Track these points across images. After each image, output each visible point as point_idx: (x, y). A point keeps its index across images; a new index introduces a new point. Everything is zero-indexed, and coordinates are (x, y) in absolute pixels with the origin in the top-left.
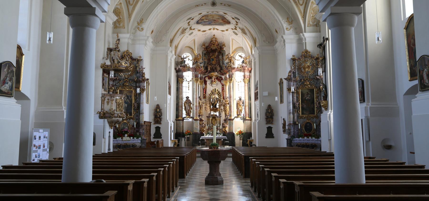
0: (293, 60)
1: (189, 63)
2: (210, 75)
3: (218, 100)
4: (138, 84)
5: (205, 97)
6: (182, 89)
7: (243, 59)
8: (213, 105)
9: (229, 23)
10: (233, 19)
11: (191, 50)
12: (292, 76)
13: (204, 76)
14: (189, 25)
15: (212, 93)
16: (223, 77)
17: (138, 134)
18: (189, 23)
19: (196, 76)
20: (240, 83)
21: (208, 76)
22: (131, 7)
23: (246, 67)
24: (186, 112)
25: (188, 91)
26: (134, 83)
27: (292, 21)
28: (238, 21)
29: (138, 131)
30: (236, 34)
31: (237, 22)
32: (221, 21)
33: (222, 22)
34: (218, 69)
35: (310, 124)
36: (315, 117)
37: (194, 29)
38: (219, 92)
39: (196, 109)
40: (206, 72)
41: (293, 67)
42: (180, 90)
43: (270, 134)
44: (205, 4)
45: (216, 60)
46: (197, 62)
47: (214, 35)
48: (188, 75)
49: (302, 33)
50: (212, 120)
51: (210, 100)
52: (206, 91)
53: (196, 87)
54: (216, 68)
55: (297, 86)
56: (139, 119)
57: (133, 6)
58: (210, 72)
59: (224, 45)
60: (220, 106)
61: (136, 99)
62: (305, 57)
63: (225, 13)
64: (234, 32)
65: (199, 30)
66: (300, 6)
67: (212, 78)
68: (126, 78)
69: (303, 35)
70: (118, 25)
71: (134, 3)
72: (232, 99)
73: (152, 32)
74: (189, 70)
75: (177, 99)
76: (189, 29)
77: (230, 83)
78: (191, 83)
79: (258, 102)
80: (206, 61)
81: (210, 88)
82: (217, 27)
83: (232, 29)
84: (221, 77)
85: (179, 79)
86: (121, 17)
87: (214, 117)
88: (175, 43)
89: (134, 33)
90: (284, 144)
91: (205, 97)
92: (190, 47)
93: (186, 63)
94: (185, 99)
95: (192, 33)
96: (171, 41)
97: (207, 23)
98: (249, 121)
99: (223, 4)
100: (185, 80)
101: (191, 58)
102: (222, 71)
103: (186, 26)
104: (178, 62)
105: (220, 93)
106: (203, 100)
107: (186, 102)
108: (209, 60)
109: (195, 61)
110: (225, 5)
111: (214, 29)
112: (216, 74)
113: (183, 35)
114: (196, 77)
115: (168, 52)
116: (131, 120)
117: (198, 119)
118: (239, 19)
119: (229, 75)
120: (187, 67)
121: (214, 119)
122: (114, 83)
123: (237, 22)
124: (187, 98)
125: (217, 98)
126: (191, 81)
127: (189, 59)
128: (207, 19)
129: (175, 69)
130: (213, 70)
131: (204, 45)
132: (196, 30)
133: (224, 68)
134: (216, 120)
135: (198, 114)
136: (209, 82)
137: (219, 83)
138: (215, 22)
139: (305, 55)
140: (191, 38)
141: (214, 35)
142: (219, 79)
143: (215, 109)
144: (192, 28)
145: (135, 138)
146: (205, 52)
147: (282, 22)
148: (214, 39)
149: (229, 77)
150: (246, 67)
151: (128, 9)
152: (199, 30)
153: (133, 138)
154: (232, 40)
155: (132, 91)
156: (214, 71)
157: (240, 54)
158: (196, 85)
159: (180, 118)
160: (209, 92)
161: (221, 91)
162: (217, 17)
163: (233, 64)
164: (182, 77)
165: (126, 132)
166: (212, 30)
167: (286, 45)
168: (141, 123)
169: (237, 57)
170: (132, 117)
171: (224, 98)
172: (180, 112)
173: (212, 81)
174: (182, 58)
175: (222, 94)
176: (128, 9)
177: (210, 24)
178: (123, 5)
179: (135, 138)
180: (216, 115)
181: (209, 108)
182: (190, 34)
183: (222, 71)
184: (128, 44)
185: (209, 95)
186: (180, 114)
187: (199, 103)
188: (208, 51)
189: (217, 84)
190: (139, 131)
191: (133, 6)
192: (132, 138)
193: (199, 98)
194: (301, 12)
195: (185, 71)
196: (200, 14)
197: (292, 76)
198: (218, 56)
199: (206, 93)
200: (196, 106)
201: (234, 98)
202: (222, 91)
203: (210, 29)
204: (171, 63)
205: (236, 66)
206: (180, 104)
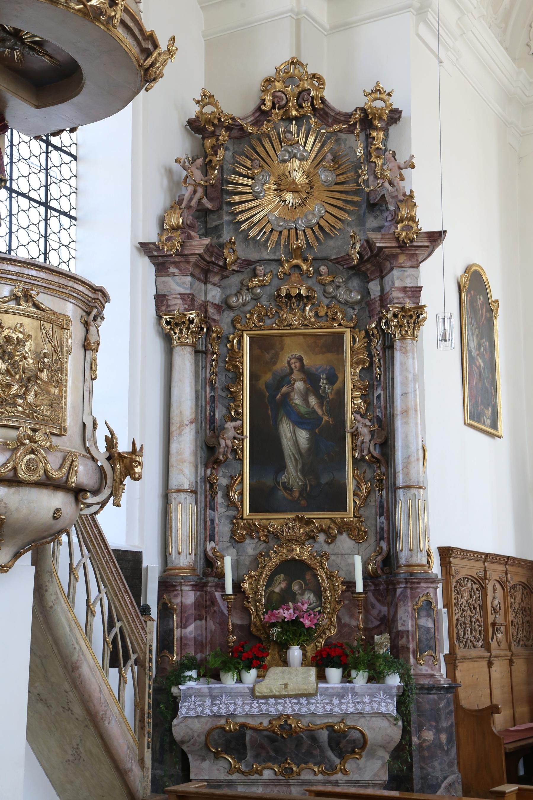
4: (374, 287)
17: (382, 642)
26: (355, 283)
29: (388, 624)
56: (388, 534)
61: (371, 388)
68: (293, 253)
116: (345, 542)
122: (214, 294)
145: (360, 679)
153: (347, 678)
155: (340, 337)
165: (295, 631)
168: (403, 557)
170: (350, 514)
179: (360, 679)
184: (298, 22)
190: (394, 620)
192: (334, 674)
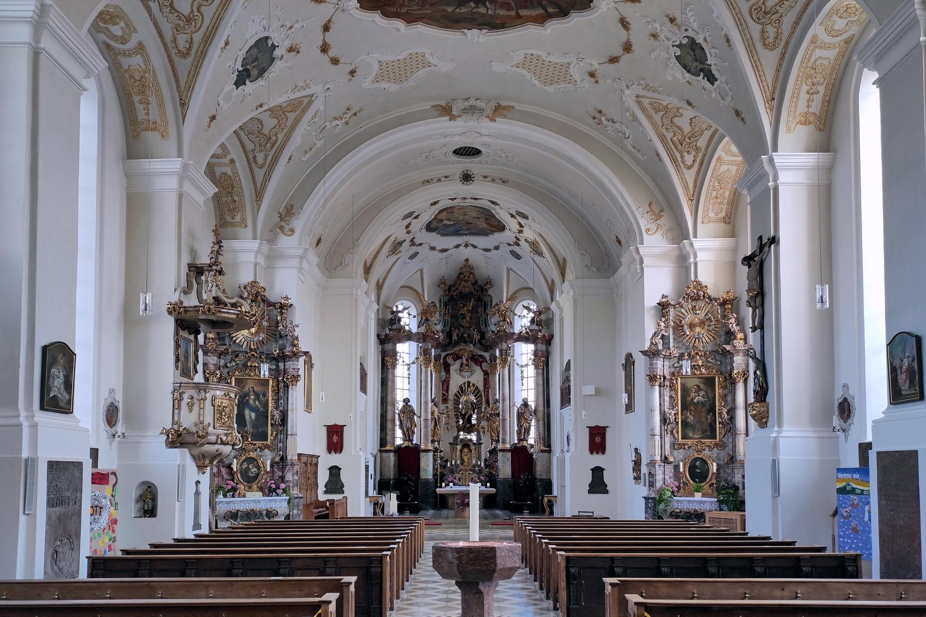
0: (663, 307)
1: (409, 321)
2: (457, 349)
3: (475, 407)
5: (445, 400)
6: (394, 382)
7: (532, 315)
8: (463, 418)
9: (501, 228)
10: (512, 216)
11: (418, 296)
12: (660, 347)
13: (443, 354)
14: (408, 232)
15: (461, 391)
16: (487, 355)
18: (407, 227)
19: (425, 352)
20: (525, 369)
22: (260, 174)
23: (540, 331)
24: (404, 434)
25: (405, 386)
27: (662, 211)
28: (523, 221)
30: (518, 257)
31: (521, 226)
32: (482, 224)
33: (485, 226)
34: (477, 337)
35: (704, 462)
36: (717, 445)
37: (421, 244)
38: (477, 388)
39: (426, 427)
40: (449, 344)
41: (662, 324)
42: (390, 384)
43: (598, 484)
44: (446, 177)
45: (471, 318)
46: (427, 320)
47: (467, 260)
48: (406, 351)
49: (687, 238)
51: (457, 408)
52: (448, 387)
53: (426, 377)
54: (470, 336)
55: (673, 370)
57: (264, 170)
58: (457, 343)
60: (478, 419)
62: (696, 298)
63: (493, 203)
64: (512, 252)
65: (433, 248)
66: (685, 170)
69: (692, 245)
70: (229, 219)
71: (268, 162)
73: (319, 241)
75: (382, 404)
76: (407, 244)
77: (503, 367)
78: (414, 368)
79: (569, 411)
80: (448, 318)
81: (456, 380)
82: (473, 240)
83: (509, 245)
84: (482, 356)
85: (387, 361)
86: (236, 198)
87: (466, 444)
88: (377, 273)
89: (272, 241)
90: (637, 512)
91: (445, 400)
92: (411, 288)
93: (402, 323)
94: (400, 405)
95: (416, 254)
96: (367, 270)
97: (451, 229)
98: (546, 454)
99: (489, 179)
100: (400, 361)
101: (414, 312)
102: (483, 341)
103: (401, 234)
104: (384, 320)
105: (479, 391)
106: (442, 407)
108: (454, 316)
109: (425, 317)
110: (493, 180)
111: (466, 246)
112: (471, 347)
113: (394, 258)
114: (425, 355)
115: (359, 293)
117: (431, 448)
118: (526, 217)
119: (501, 351)
120: (404, 331)
123: (521, 226)
124: (406, 401)
125: (472, 403)
126: (414, 363)
127: (409, 314)
128: (449, 220)
129: (378, 336)
130: (462, 340)
132: (426, 247)
133: (489, 335)
134: (470, 451)
136: (455, 367)
137: (477, 369)
138: (469, 226)
139: (693, 293)
140: (416, 264)
141: (467, 260)
142: (477, 360)
143: (469, 429)
144: (417, 241)
146: (446, 299)
147: (636, 213)
149: (501, 354)
150: (540, 331)
151: (253, 178)
152: (433, 248)
154: (508, 270)
156: (465, 342)
157: (525, 303)
158: (426, 372)
159: (388, 448)
161: (481, 388)
162: (474, 214)
163: (511, 324)
164: (394, 354)
166: (462, 248)
167: (646, 271)
169: (519, 310)
171: (488, 403)
172: (389, 433)
173: (462, 365)
174: (393, 313)
175: (484, 394)
176: (253, 178)
177: (457, 233)
178: (237, 164)
180: (471, 440)
182: (412, 257)
183: (483, 341)
186: (389, 438)
187: (432, 414)
188: (452, 296)
189: (472, 372)
191: (264, 170)
193: (433, 401)
194: (686, 187)
195: (400, 341)
196: (434, 204)
197: (660, 347)
199: (447, 391)
200: (426, 420)
203: (457, 246)
204: (367, 320)
205: (517, 330)
206: (389, 416)
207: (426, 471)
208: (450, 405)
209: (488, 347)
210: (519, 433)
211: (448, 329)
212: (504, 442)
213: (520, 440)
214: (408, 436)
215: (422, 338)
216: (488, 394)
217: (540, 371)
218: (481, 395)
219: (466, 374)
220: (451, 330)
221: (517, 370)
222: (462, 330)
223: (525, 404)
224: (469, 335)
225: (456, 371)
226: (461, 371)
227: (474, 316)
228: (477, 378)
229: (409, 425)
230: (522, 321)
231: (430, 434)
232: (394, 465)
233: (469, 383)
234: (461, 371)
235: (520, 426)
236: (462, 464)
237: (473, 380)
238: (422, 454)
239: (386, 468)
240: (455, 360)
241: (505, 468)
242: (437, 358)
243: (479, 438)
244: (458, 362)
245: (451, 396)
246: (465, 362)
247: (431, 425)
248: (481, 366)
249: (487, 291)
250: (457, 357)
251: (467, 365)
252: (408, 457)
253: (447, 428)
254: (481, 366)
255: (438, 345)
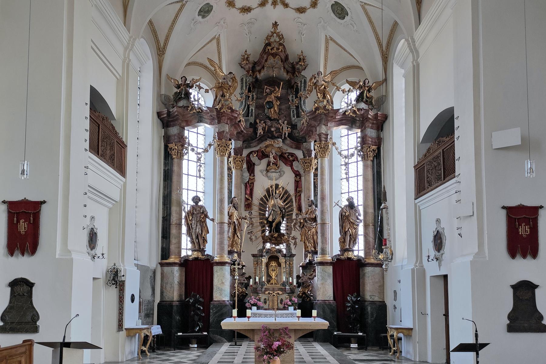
1: (202, 98)
2: (263, 145)
3: (285, 213)
5: (248, 206)
8: (270, 226)
15: (269, 194)
21: (257, 151)
24: (192, 242)
34: (286, 130)
38: (286, 192)
39: (221, 232)
42: (175, 178)
48: (199, 136)
50: (267, 265)
58: (262, 139)
59: (302, 59)
60: (288, 228)
67: (268, 156)
72: (327, 202)
74: (201, 120)
75: (164, 204)
81: (262, 183)
84: (292, 155)
87: (274, 257)
91: (248, 206)
98: (378, 269)
102: (296, 133)
105: (289, 195)
106: (245, 214)
107: (190, 213)
108: (260, 107)
109: (222, 89)
112: (279, 143)
114: (220, 139)
121: (273, 264)
124: (196, 200)
130: (269, 135)
131: (246, 58)
134: (279, 265)
135: (226, 249)
137: (287, 169)
143: (277, 238)
148: (275, 38)
156: (273, 137)
158: (222, 162)
159: (172, 260)
160: (259, 192)
161: (292, 192)
171: (300, 209)
172: (173, 241)
173: (269, 164)
180: (280, 251)
181: (259, 234)
185: (262, 199)
186: (173, 247)
187: (230, 216)
193: (231, 201)
198: (282, 99)
200: (221, 223)
201: (335, 200)
202: (296, 190)
206: (174, 219)
207: (221, 290)
208: (255, 210)
209: (298, 141)
210: (342, 241)
211: (252, 119)
212: (324, 253)
213: (344, 250)
214: (199, 242)
215: (218, 115)
216: (300, 200)
217: (369, 163)
218: (291, 201)
219: (274, 175)
220: (256, 123)
221: (338, 160)
222: (269, 123)
223: (351, 206)
224: (278, 130)
225: (261, 171)
226: (267, 171)
227: (283, 107)
228: (286, 180)
229: (198, 230)
230: (344, 100)
231: (226, 242)
232: (180, 284)
233: (277, 186)
234: (267, 171)
235: (343, 232)
236: (268, 281)
237: (281, 183)
238: (216, 268)
239: (168, 287)
240: (260, 158)
241: (324, 287)
242: (238, 151)
243: (288, 247)
244: (265, 161)
245: (256, 201)
246: (272, 160)
247: (228, 231)
248: (291, 166)
249: (300, 72)
250: (263, 155)
251: (275, 164)
252: (198, 272)
253: (251, 239)
254: (291, 166)
255: (239, 135)
